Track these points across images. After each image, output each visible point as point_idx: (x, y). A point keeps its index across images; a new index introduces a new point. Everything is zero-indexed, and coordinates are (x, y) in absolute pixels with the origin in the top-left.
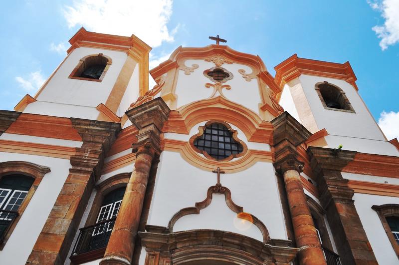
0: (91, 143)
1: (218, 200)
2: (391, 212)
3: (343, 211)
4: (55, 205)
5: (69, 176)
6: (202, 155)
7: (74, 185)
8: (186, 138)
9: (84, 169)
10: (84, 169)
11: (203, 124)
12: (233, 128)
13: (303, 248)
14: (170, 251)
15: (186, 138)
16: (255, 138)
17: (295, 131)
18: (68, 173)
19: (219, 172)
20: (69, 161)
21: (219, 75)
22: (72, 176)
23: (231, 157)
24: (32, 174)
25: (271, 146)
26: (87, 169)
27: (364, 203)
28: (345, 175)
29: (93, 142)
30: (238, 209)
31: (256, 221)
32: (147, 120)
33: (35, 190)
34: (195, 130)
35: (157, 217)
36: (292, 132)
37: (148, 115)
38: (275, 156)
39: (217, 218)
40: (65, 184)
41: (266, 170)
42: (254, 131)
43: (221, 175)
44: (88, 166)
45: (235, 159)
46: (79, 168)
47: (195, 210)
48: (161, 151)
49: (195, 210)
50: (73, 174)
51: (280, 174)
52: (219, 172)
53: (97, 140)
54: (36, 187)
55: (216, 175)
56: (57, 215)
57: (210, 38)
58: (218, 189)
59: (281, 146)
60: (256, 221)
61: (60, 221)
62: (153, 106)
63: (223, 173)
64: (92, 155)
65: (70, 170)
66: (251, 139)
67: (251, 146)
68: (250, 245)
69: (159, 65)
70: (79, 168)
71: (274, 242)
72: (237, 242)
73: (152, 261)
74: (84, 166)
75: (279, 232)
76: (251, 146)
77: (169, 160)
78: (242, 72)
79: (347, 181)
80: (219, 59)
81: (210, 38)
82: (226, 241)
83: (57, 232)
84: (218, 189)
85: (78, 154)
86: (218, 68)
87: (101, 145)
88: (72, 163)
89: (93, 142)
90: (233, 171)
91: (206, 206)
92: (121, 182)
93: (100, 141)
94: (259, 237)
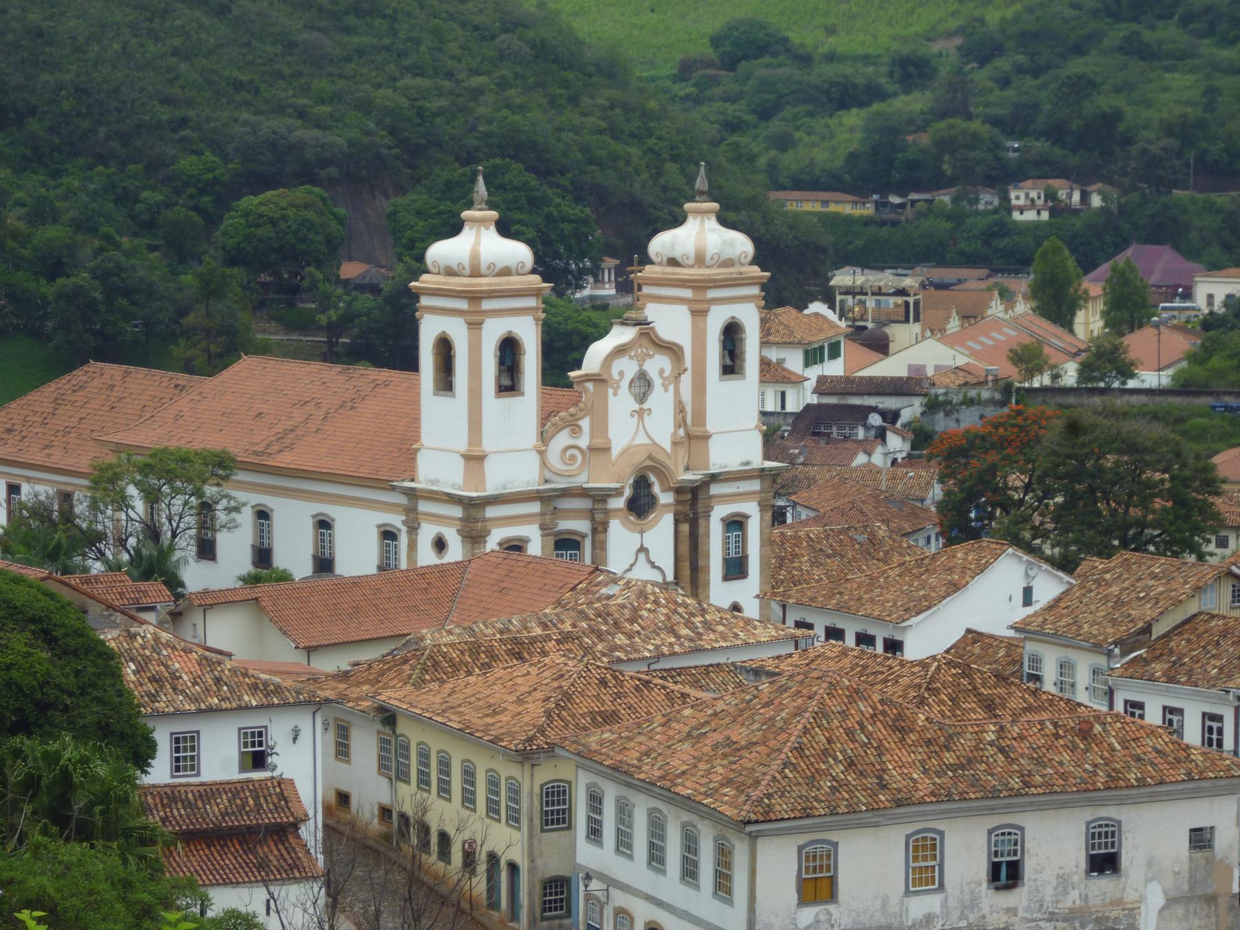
1: (642, 556)
3: (701, 531)
11: (631, 481)
12: (653, 478)
15: (619, 503)
16: (666, 489)
19: (642, 532)
21: (642, 385)
27: (719, 512)
41: (668, 520)
47: (630, 569)
49: (630, 569)
51: (677, 522)
55: (639, 536)
58: (642, 549)
75: (670, 577)
76: (665, 498)
78: (661, 372)
84: (642, 549)
90: (650, 528)
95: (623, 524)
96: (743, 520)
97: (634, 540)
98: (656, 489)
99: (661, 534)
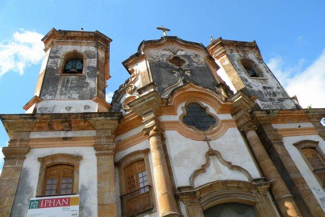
0: (102, 130)
2: (303, 146)
3: (279, 151)
4: (98, 183)
5: (98, 159)
6: (191, 129)
7: (105, 165)
8: (176, 118)
9: (106, 152)
10: (106, 152)
11: (183, 105)
12: (205, 104)
13: (272, 180)
14: (198, 200)
15: (176, 118)
16: (223, 110)
17: (246, 102)
18: (95, 158)
20: (93, 148)
22: (100, 159)
23: (211, 127)
24: (70, 162)
25: (232, 115)
26: (108, 152)
27: (289, 142)
28: (275, 126)
29: (104, 129)
30: (229, 163)
31: (239, 169)
32: (146, 109)
33: (78, 174)
34: (180, 111)
35: (182, 180)
36: (244, 103)
37: (147, 105)
38: (237, 121)
39: (217, 173)
40: (98, 166)
42: (220, 106)
43: (211, 143)
44: (108, 150)
45: (214, 129)
46: (102, 152)
47: (202, 170)
48: (164, 131)
49: (202, 170)
50: (101, 157)
51: (244, 134)
52: (207, 140)
53: (106, 127)
54: (78, 172)
55: (205, 143)
56: (104, 190)
57: (157, 28)
58: (212, 153)
59: (239, 114)
60: (239, 169)
61: (107, 194)
62: (151, 97)
63: (210, 140)
64: (108, 140)
65: (96, 155)
66: (220, 110)
67: (222, 117)
68: (243, 186)
69: (139, 64)
70: (102, 152)
71: (256, 180)
72: (236, 185)
73: (190, 209)
74: (106, 150)
75: (256, 174)
77: (171, 135)
79: (276, 130)
80: (175, 47)
81: (157, 28)
82: (229, 187)
83: (109, 202)
84: (212, 153)
85: (97, 140)
86: (175, 55)
87: (110, 131)
88: (96, 149)
89: (104, 129)
91: (208, 166)
92: (137, 158)
93: (109, 127)
94: (246, 179)
95: (180, 132)
96: (315, 145)
97: (203, 147)
98: (212, 110)
99: (231, 142)
